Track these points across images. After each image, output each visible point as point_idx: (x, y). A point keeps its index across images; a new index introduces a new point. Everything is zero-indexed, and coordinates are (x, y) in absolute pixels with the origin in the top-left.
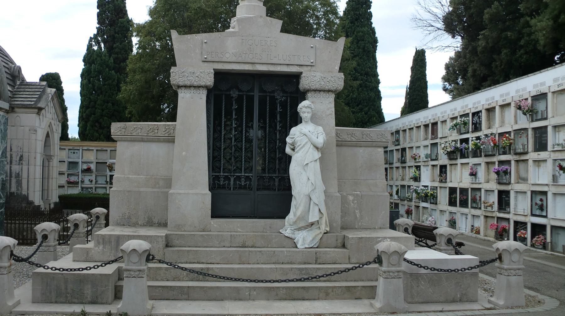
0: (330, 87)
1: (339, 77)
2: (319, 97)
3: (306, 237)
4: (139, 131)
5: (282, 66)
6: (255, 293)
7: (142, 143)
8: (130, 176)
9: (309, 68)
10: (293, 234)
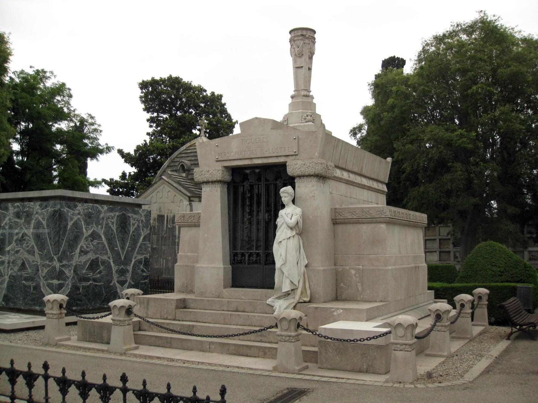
5: (272, 158)
6: (213, 346)
8: (188, 254)
9: (294, 157)
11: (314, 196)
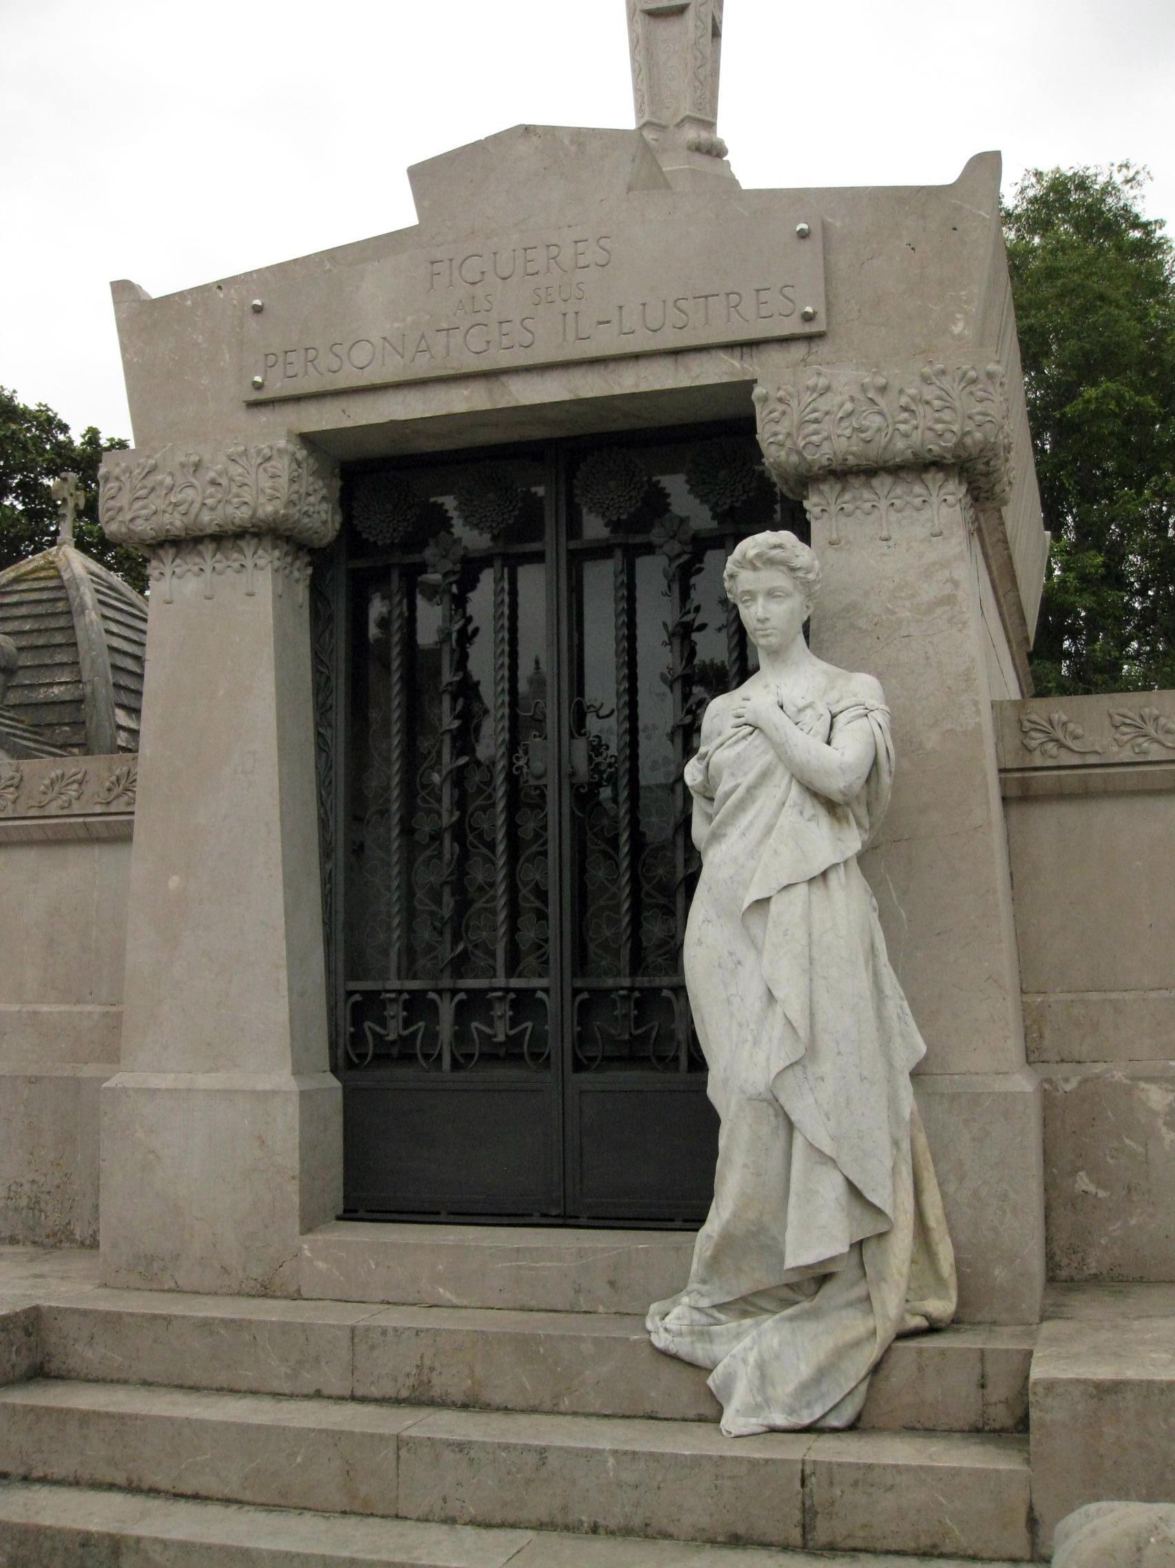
0: (916, 437)
1: (972, 374)
3: (777, 1357)
4: (72, 791)
7: (97, 851)
8: (45, 1008)
9: (798, 351)
10: (703, 1335)
11: (949, 600)
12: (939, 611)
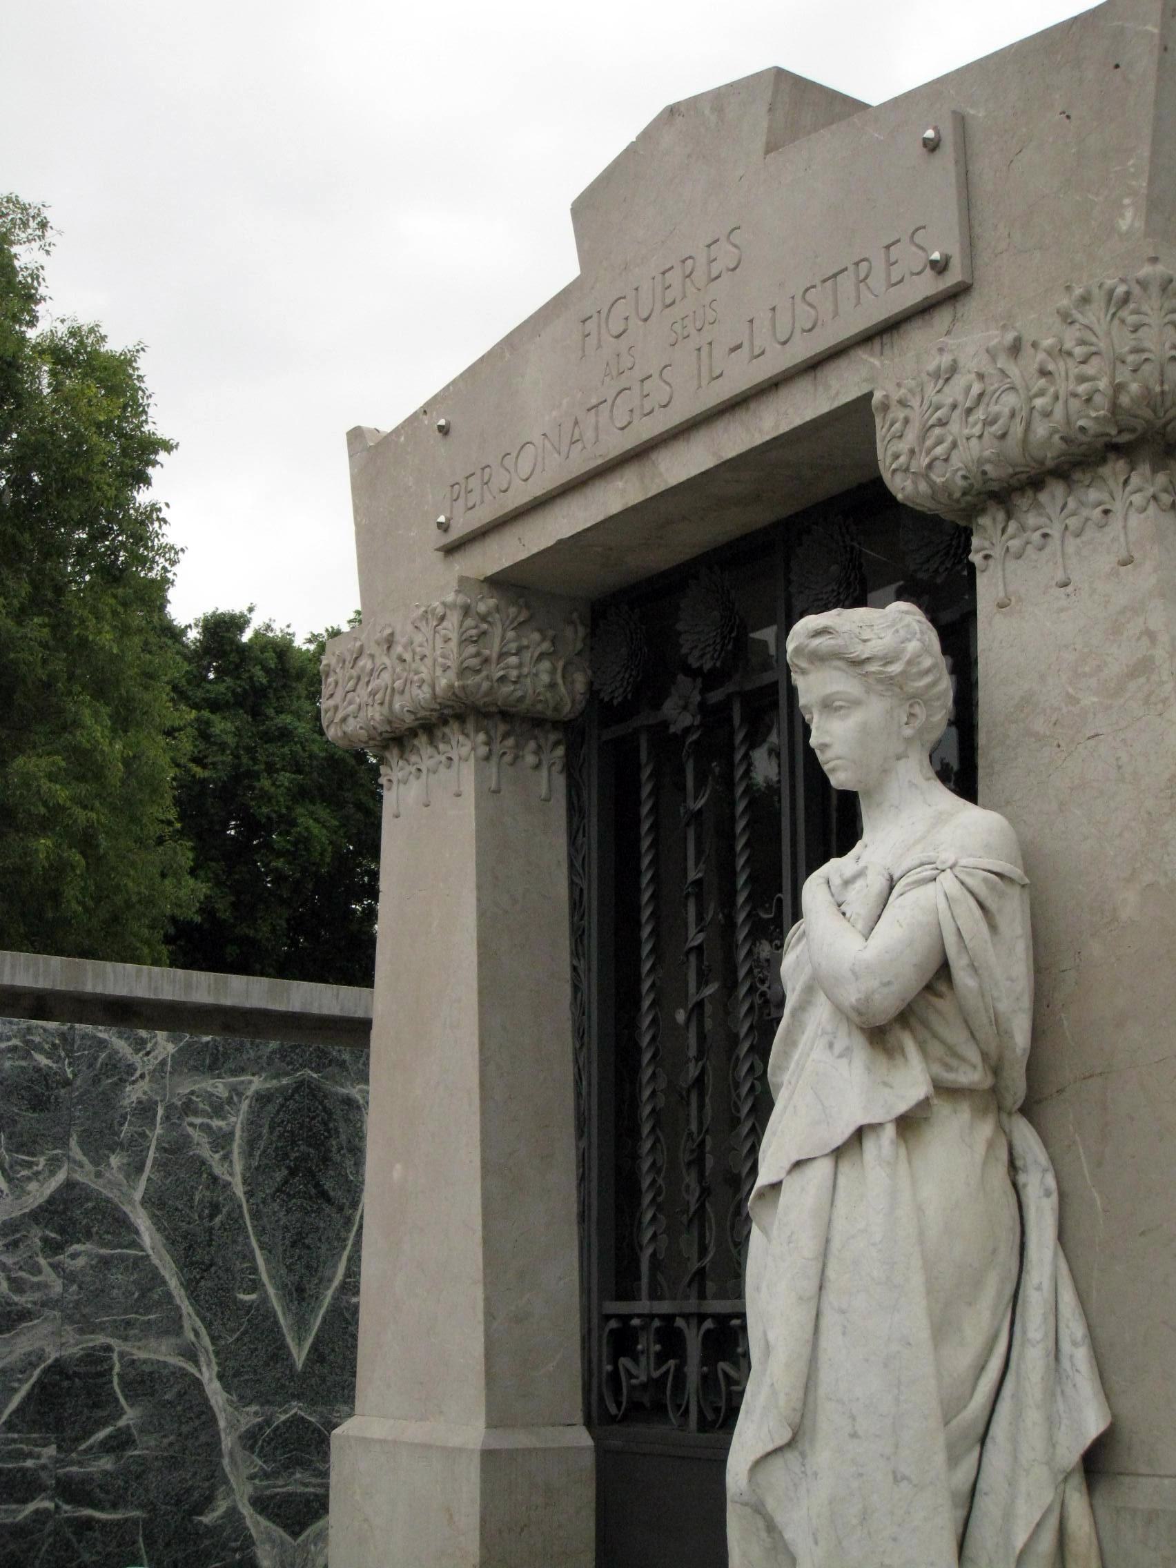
2: (1036, 536)
11: (1144, 667)
12: (1132, 686)
